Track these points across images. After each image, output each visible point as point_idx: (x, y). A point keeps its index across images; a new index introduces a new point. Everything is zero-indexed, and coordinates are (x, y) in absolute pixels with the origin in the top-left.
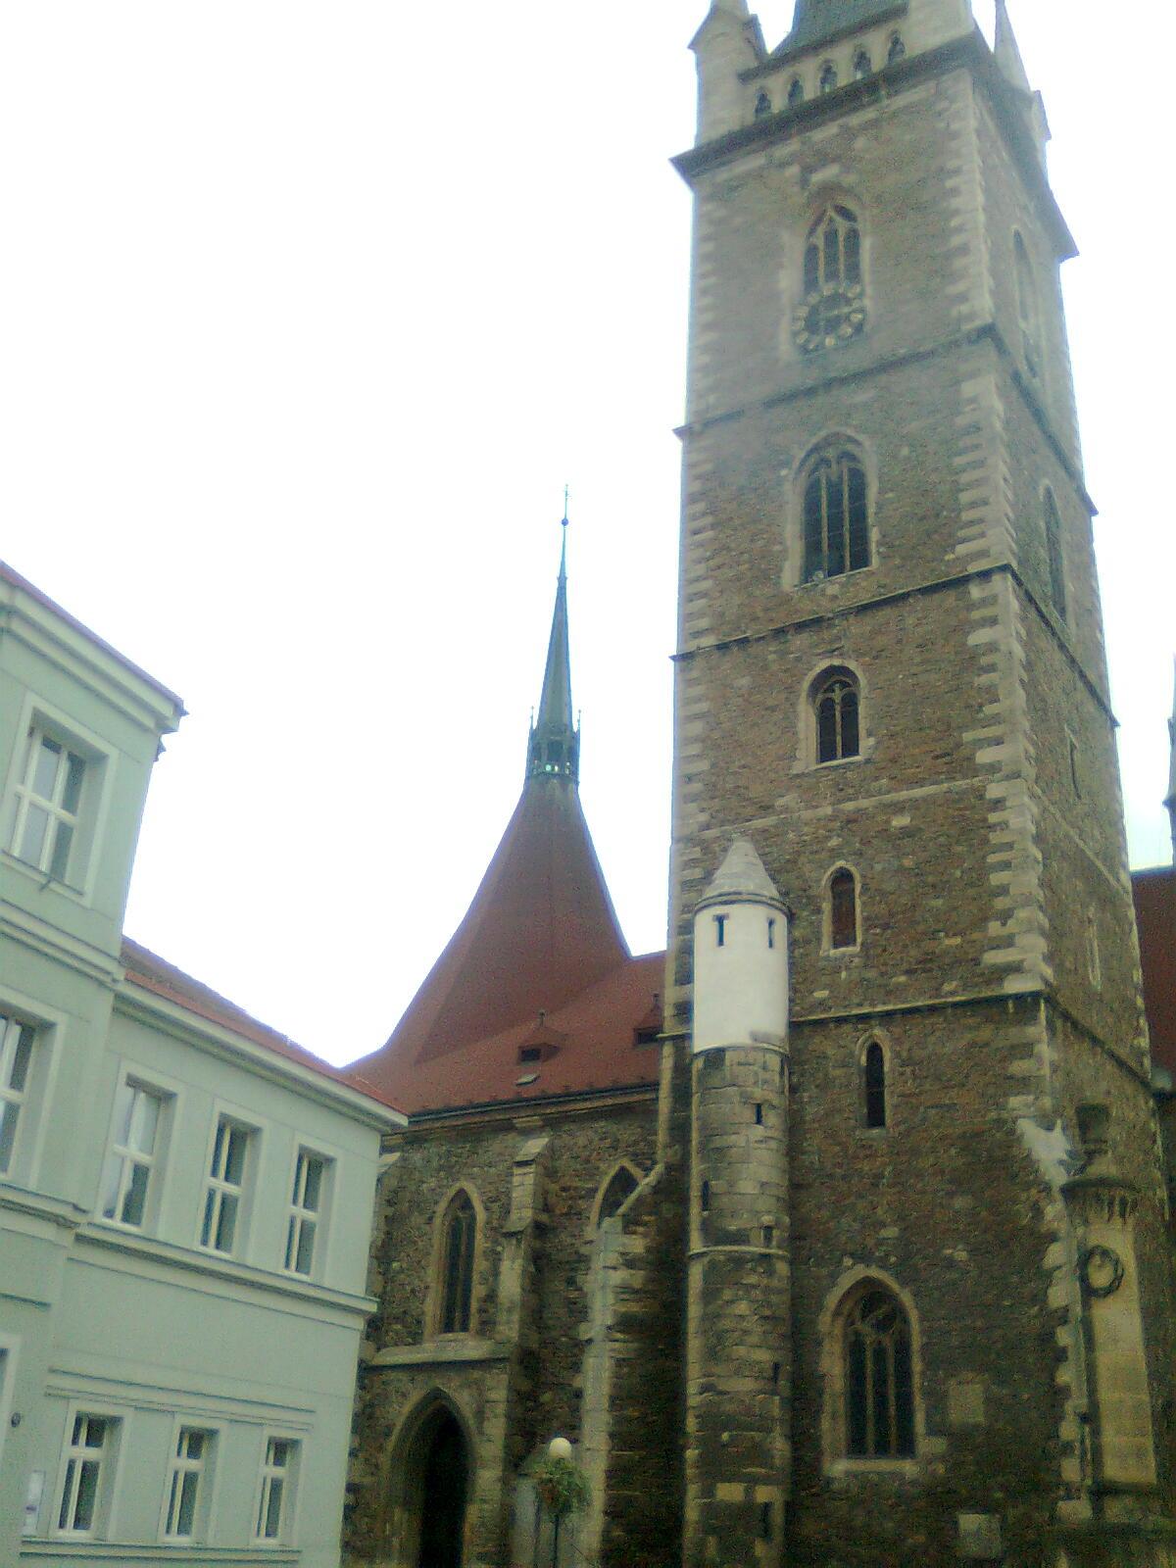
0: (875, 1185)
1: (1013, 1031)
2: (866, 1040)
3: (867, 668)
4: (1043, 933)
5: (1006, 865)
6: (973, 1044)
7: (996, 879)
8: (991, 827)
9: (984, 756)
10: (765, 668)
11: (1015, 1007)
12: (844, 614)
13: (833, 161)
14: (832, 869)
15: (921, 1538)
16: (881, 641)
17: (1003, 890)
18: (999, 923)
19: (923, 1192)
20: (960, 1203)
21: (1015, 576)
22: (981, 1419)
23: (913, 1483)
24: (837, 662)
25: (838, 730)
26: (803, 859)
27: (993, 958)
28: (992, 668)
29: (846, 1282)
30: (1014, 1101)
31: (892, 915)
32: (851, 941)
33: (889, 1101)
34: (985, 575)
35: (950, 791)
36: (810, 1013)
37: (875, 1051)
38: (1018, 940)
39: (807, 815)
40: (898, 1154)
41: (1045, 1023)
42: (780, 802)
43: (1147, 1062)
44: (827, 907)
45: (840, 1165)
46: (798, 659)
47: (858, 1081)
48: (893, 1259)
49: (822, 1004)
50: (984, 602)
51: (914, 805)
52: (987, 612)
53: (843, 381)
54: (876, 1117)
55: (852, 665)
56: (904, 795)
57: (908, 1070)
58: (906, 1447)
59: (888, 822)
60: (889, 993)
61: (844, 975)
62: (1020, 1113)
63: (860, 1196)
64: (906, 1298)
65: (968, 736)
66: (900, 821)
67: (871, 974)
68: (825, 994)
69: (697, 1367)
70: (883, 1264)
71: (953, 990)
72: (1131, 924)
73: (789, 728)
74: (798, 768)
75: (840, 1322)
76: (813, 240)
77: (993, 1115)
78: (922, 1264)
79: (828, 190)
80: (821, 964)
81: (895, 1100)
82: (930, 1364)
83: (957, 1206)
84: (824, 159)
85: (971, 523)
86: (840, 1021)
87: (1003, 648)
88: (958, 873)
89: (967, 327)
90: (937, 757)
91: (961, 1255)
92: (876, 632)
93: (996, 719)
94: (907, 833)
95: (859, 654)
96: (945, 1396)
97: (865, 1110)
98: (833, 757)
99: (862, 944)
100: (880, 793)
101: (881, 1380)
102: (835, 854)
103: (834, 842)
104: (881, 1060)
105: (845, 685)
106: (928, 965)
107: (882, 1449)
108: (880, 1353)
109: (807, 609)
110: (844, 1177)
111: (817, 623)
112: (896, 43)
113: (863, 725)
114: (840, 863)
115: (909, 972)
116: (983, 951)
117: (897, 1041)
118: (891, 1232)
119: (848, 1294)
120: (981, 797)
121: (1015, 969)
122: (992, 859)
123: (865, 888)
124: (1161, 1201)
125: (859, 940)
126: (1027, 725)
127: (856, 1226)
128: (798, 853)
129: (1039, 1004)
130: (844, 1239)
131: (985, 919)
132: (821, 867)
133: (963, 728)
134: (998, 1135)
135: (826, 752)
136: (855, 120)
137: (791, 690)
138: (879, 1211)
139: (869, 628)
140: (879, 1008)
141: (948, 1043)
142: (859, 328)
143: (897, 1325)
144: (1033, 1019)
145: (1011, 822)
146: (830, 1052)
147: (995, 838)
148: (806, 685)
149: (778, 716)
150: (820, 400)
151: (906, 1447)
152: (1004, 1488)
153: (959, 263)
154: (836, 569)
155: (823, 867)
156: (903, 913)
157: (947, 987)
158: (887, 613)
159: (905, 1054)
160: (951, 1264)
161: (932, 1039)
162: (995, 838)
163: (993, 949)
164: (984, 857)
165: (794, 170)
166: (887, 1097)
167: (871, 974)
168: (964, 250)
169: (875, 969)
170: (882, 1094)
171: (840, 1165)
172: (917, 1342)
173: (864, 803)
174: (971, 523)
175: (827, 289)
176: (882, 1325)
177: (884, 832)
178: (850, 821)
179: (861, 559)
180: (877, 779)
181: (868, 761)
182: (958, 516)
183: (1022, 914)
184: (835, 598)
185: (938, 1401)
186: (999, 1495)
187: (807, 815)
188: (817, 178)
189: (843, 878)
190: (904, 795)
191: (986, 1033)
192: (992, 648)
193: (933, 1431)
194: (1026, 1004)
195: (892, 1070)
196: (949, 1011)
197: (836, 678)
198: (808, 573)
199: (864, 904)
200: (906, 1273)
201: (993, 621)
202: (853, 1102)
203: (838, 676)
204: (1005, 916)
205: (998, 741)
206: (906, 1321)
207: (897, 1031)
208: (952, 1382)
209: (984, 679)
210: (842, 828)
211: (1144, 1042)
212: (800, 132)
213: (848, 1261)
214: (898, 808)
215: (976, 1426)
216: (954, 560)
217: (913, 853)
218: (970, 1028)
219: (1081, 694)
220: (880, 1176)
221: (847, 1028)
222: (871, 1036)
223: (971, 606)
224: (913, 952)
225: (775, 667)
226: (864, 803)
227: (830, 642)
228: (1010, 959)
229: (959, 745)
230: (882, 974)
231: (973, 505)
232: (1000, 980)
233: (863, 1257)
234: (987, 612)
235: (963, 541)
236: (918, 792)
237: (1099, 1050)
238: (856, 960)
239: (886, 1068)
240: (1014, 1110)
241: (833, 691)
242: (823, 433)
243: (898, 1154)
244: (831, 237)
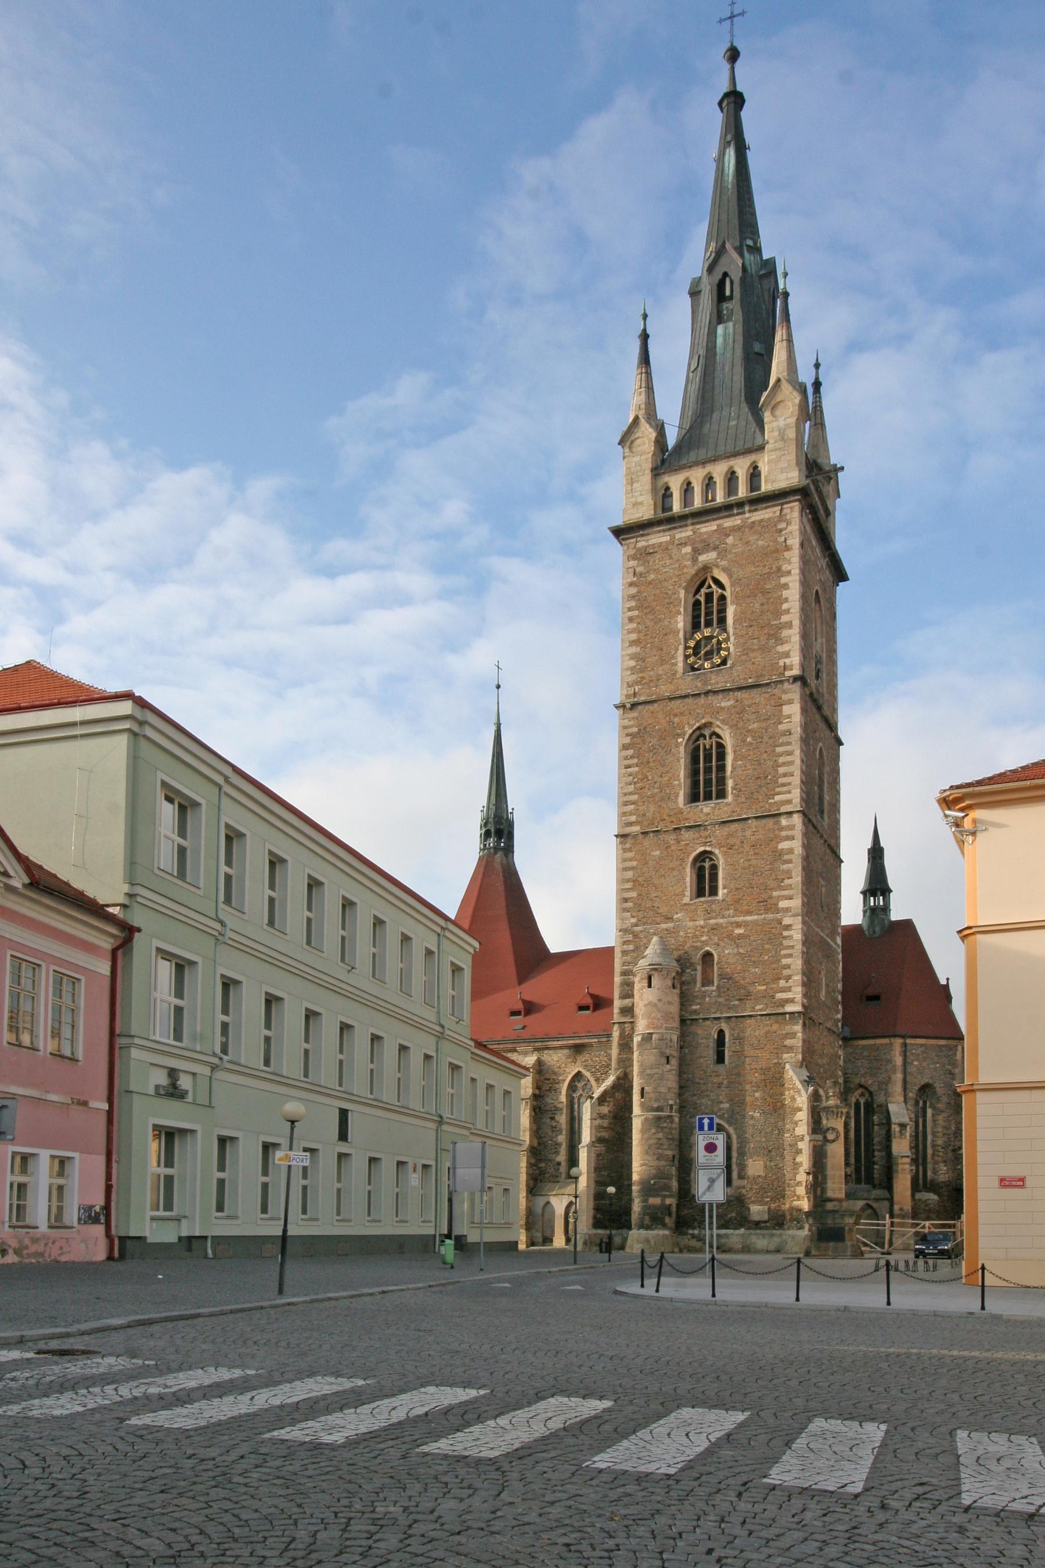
3: (725, 854)
12: (713, 824)
24: (708, 849)
51: (746, 924)
53: (715, 692)
55: (717, 851)
56: (741, 919)
60: (729, 1008)
69: (638, 1158)
76: (698, 597)
79: (706, 568)
84: (707, 547)
95: (720, 846)
150: (702, 700)
154: (708, 797)
157: (757, 1007)
165: (688, 549)
173: (721, 921)
175: (707, 632)
177: (730, 936)
179: (721, 794)
181: (723, 900)
184: (708, 814)
188: (703, 558)
190: (741, 919)
207: (732, 1024)
212: (693, 524)
214: (738, 925)
226: (721, 921)
227: (706, 838)
242: (703, 721)
244: (709, 597)
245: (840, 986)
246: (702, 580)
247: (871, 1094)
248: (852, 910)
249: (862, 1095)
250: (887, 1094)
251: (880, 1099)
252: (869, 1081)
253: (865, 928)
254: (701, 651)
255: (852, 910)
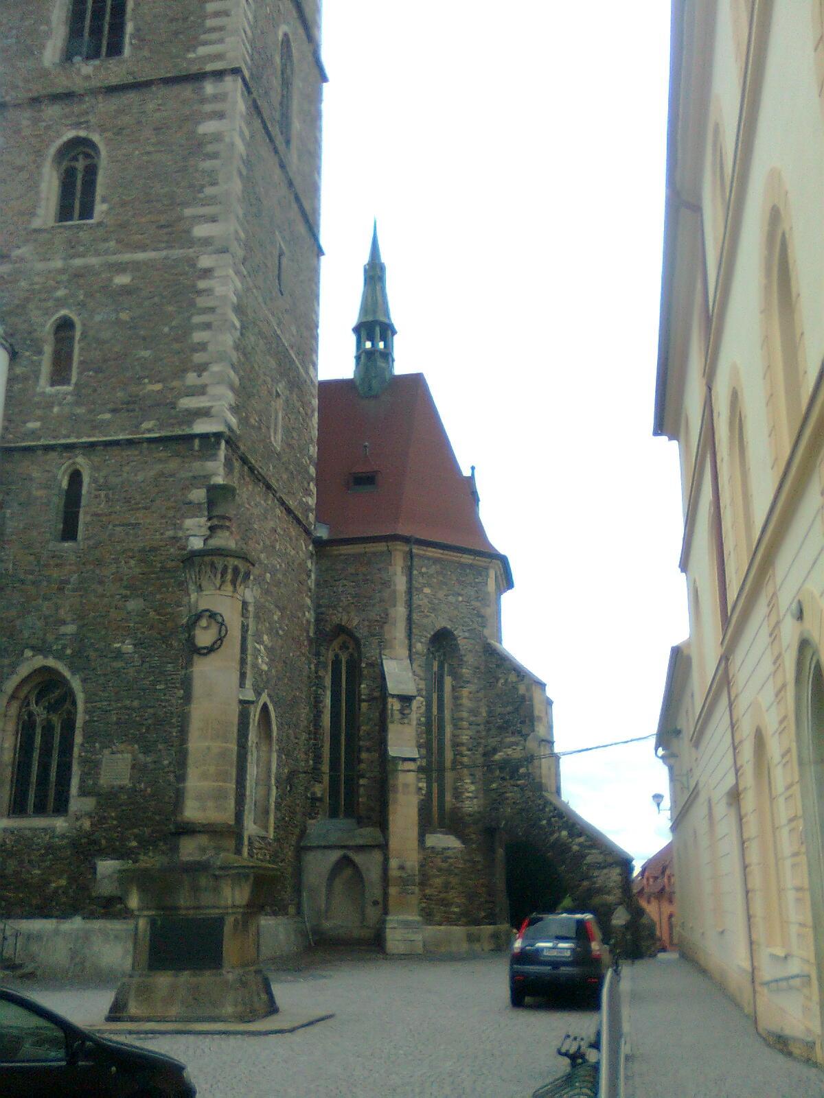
0: (61, 589)
1: (197, 465)
2: (70, 466)
3: (108, 142)
4: (232, 388)
5: (207, 326)
6: (162, 474)
7: (198, 336)
8: (199, 293)
9: (200, 231)
10: (18, 132)
11: (201, 446)
12: (94, 92)
14: (57, 316)
15: (63, 882)
16: (126, 119)
17: (203, 347)
18: (195, 374)
19: (103, 596)
20: (133, 605)
21: (244, 79)
22: (126, 782)
23: (63, 836)
24: (82, 134)
25: (76, 196)
26: (31, 306)
27: (187, 403)
28: (215, 156)
29: (24, 670)
30: (189, 523)
31: (105, 361)
32: (65, 381)
33: (83, 518)
34: (219, 75)
35: (166, 258)
36: (23, 440)
37: (76, 477)
38: (210, 390)
39: (40, 266)
40: (84, 564)
41: (223, 460)
42: (16, 253)
43: (312, 517)
44: (48, 349)
45: (32, 572)
46: (48, 128)
47: (58, 502)
48: (69, 651)
49: (33, 432)
50: (216, 98)
51: (135, 267)
52: (218, 107)
54: (69, 532)
55: (96, 138)
56: (127, 257)
57: (103, 493)
58: (61, 807)
59: (110, 280)
60: (94, 428)
61: (56, 410)
62: (192, 533)
63: (45, 598)
64: (76, 684)
65: (188, 212)
66: (122, 280)
67: (80, 411)
68: (38, 424)
70: (59, 656)
71: (150, 428)
72: (313, 411)
73: (33, 186)
74: (37, 223)
75: (15, 705)
77: (170, 533)
78: (93, 654)
80: (36, 399)
81: (88, 518)
82: (89, 737)
83: (130, 608)
85: (213, 30)
86: (48, 448)
87: (227, 139)
88: (166, 329)
90: (162, 227)
91: (128, 648)
92: (120, 112)
93: (212, 200)
94: (126, 291)
95: (102, 129)
96: (96, 765)
97: (61, 526)
98: (71, 219)
99: (76, 384)
100: (106, 252)
101: (46, 751)
102: (61, 303)
103: (60, 293)
104: (80, 483)
105: (87, 156)
106: (133, 406)
107: (40, 810)
108: (48, 729)
109: (62, 83)
110: (33, 583)
111: (67, 96)
113: (100, 191)
114: (63, 312)
115: (114, 411)
116: (180, 396)
117: (96, 469)
118: (70, 629)
119: (24, 681)
120: (194, 266)
121: (205, 413)
122: (197, 319)
123: (84, 335)
124: (308, 622)
125: (74, 380)
126: (241, 212)
127: (39, 624)
128: (27, 300)
129: (219, 444)
130: (26, 635)
131: (185, 371)
132: (47, 314)
133: (185, 204)
134: (172, 550)
135: (65, 213)
137: (39, 153)
138: (62, 612)
139: (114, 107)
140: (84, 440)
141: (141, 472)
143: (67, 706)
144: (213, 457)
145: (217, 289)
146: (35, 475)
147: (201, 302)
148: (52, 150)
149: (24, 175)
151: (61, 807)
152: (136, 837)
154: (94, 54)
155: (47, 313)
156: (115, 359)
157: (145, 426)
158: (132, 96)
159: (101, 481)
160: (119, 654)
161: (126, 469)
162: (201, 302)
163: (187, 396)
164: (189, 318)
166: (81, 516)
167: (80, 411)
169: (84, 407)
170: (78, 512)
171: (32, 572)
172: (79, 723)
173: (93, 261)
174: (213, 30)
176: (51, 708)
177: (104, 288)
178: (78, 275)
179: (115, 49)
180: (106, 240)
181: (100, 224)
182: (203, 21)
183: (215, 368)
184: (87, 78)
185: (92, 767)
186: (134, 844)
187: (40, 266)
189: (65, 325)
190: (127, 257)
191: (173, 465)
192: (217, 137)
193: (83, 793)
194: (210, 441)
195: (89, 492)
196: (145, 445)
197: (81, 149)
198: (68, 56)
199: (82, 349)
200: (78, 662)
201: (220, 115)
202: (52, 519)
203: (79, 148)
204: (201, 369)
205: (213, 219)
206: (74, 703)
207: (96, 459)
208: (106, 752)
209: (208, 164)
210: (69, 281)
211: (312, 501)
213: (28, 653)
214: (121, 268)
215: (121, 788)
216: (195, 59)
217: (130, 309)
218: (160, 461)
219: (294, 213)
220: (67, 582)
221: (53, 455)
222: (74, 463)
223: (203, 101)
224: (120, 394)
225: (26, 132)
226: (93, 261)
228: (202, 405)
229: (180, 218)
230: (90, 411)
231: (217, 14)
232: (190, 423)
233: (41, 649)
234: (218, 107)
235: (205, 43)
236: (141, 256)
237: (271, 495)
238: (69, 397)
239: (84, 491)
240: (188, 530)
241: (77, 160)
243: (84, 564)
245: (313, 450)
247: (357, 642)
248: (336, 360)
249: (344, 647)
250: (383, 644)
251: (370, 652)
252: (354, 620)
253: (358, 383)
255: (336, 360)
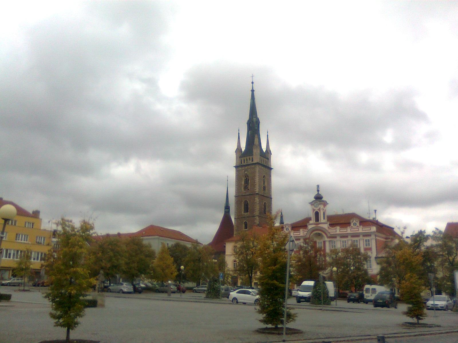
13: (247, 171)
25: (246, 227)
34: (256, 216)
79: (246, 174)
89: (256, 193)
112: (252, 159)
136: (249, 167)
142: (248, 189)
153: (256, 186)
154: (246, 212)
168: (256, 185)
192: (256, 222)
203: (246, 222)
244: (247, 178)
246: (246, 176)
254: (246, 188)
